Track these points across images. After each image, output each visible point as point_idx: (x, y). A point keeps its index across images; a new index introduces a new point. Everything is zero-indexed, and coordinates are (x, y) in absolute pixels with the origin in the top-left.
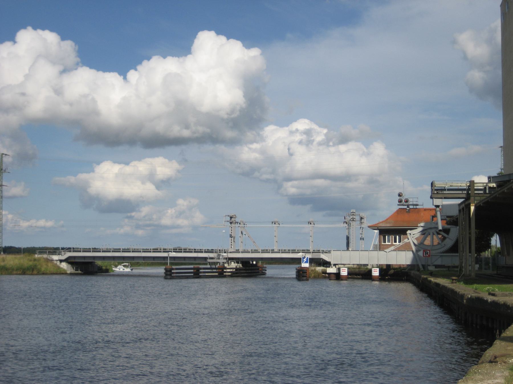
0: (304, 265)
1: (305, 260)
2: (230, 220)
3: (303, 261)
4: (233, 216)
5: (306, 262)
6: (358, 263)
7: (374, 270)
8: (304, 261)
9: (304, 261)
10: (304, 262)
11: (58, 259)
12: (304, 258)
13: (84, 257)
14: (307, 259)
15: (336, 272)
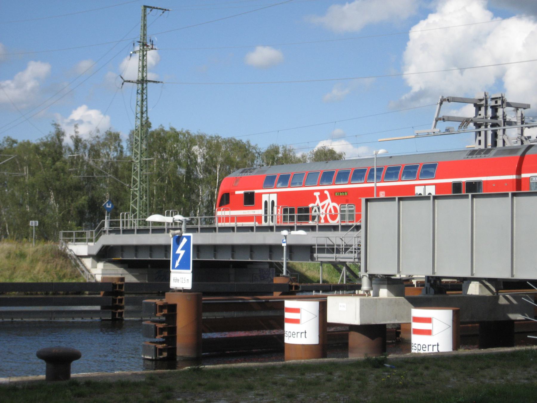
0: (177, 280)
1: (181, 252)
2: (475, 116)
3: (176, 256)
4: (481, 100)
5: (183, 266)
6: (505, 275)
7: (418, 320)
8: (179, 255)
9: (179, 255)
10: (177, 264)
11: (86, 254)
12: (178, 240)
13: (234, 248)
14: (186, 247)
15: (286, 318)
